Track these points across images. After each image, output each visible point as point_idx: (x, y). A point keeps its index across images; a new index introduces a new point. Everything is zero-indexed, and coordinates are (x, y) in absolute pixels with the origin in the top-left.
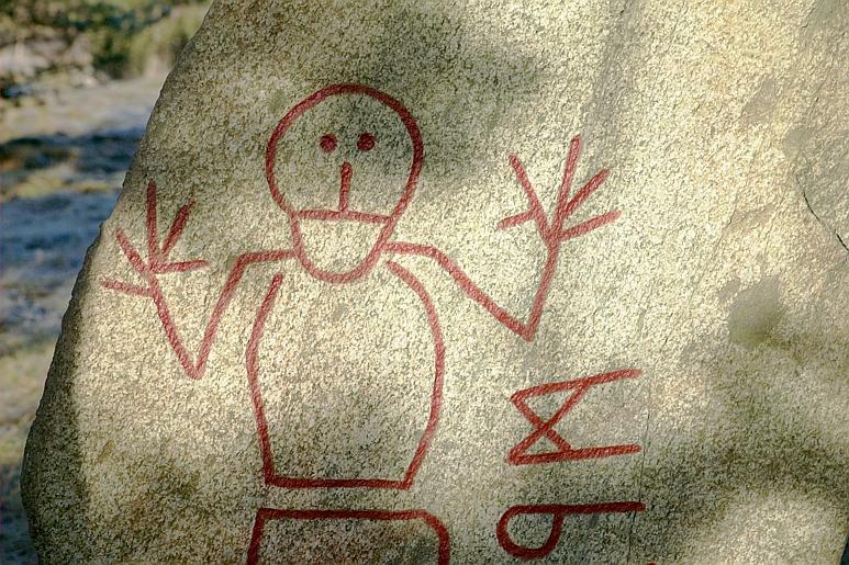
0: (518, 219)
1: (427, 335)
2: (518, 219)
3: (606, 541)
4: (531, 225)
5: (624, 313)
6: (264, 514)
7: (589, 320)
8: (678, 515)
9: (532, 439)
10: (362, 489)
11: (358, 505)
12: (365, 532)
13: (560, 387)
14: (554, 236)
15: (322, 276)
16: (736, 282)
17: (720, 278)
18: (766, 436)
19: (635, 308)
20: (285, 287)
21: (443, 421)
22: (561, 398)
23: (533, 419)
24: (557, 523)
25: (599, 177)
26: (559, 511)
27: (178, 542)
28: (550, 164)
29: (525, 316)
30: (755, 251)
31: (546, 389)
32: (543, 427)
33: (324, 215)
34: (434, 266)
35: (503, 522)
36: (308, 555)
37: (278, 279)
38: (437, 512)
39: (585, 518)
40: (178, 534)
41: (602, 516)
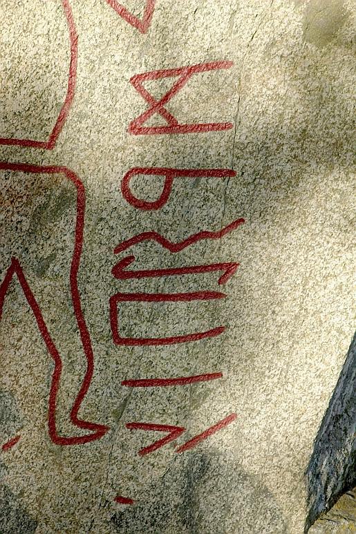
1: (63, 24)
3: (206, 199)
5: (218, 12)
7: (191, 18)
8: (262, 181)
9: (148, 114)
10: (16, 147)
11: (13, 159)
12: (20, 181)
13: (170, 73)
18: (332, 120)
19: (227, 9)
21: (77, 96)
22: (170, 82)
23: (149, 98)
24: (168, 185)
26: (170, 174)
29: (140, 12)
31: (159, 75)
35: (126, 178)
38: (75, 169)
39: (190, 180)
41: (203, 179)
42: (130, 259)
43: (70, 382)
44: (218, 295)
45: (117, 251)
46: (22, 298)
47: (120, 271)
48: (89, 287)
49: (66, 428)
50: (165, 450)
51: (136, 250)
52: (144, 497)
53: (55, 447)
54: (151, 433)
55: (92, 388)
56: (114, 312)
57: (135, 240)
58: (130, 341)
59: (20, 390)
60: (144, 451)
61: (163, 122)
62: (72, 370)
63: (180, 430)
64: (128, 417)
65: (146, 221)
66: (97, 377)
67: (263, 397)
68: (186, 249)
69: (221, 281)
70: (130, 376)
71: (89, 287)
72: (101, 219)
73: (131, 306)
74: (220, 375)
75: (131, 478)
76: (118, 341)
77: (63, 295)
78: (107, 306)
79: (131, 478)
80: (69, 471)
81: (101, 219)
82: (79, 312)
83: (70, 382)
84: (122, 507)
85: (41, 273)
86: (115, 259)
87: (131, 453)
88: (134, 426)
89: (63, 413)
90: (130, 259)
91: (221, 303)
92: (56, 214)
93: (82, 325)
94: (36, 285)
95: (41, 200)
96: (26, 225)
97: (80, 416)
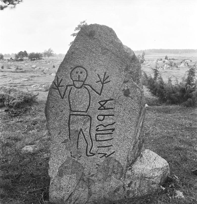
0: (99, 81)
1: (88, 95)
2: (99, 81)
3: (110, 119)
4: (100, 82)
6: (70, 115)
14: (103, 84)
15: (76, 88)
16: (124, 89)
17: (122, 89)
19: (112, 92)
20: (72, 89)
24: (104, 117)
25: (108, 77)
26: (104, 116)
27: (61, 117)
28: (102, 75)
29: (99, 92)
30: (126, 85)
32: (102, 106)
33: (77, 81)
34: (89, 87)
36: (75, 120)
37: (71, 88)
39: (107, 117)
40: (61, 116)
41: (109, 116)
42: (98, 128)
43: (89, 147)
44: (112, 134)
45: (96, 127)
46: (82, 134)
47: (97, 130)
48: (92, 133)
49: (89, 154)
50: (104, 157)
51: (99, 127)
52: (101, 164)
53: (87, 157)
54: (102, 155)
55: (93, 148)
56: (96, 136)
57: (99, 126)
58: (98, 141)
59: (82, 148)
60: (101, 157)
61: (103, 108)
62: (90, 145)
63: (107, 154)
64: (98, 152)
65: (101, 123)
66: (93, 146)
67: (119, 149)
68: (107, 127)
69: (112, 131)
70: (98, 146)
71: (92, 133)
72: (94, 122)
73: (99, 135)
74: (112, 146)
75: (99, 162)
76: (97, 141)
77: (88, 134)
78: (95, 135)
79: (99, 162)
80: (89, 160)
81: (94, 122)
82: (91, 136)
83: (89, 147)
84: (97, 166)
85: (85, 131)
86: (96, 128)
87: (99, 158)
88: (99, 154)
89: (88, 152)
90: (98, 128)
91: (112, 135)
92: (87, 122)
93: (91, 138)
94: (84, 132)
95: (85, 120)
96: (83, 123)
97: (91, 152)
